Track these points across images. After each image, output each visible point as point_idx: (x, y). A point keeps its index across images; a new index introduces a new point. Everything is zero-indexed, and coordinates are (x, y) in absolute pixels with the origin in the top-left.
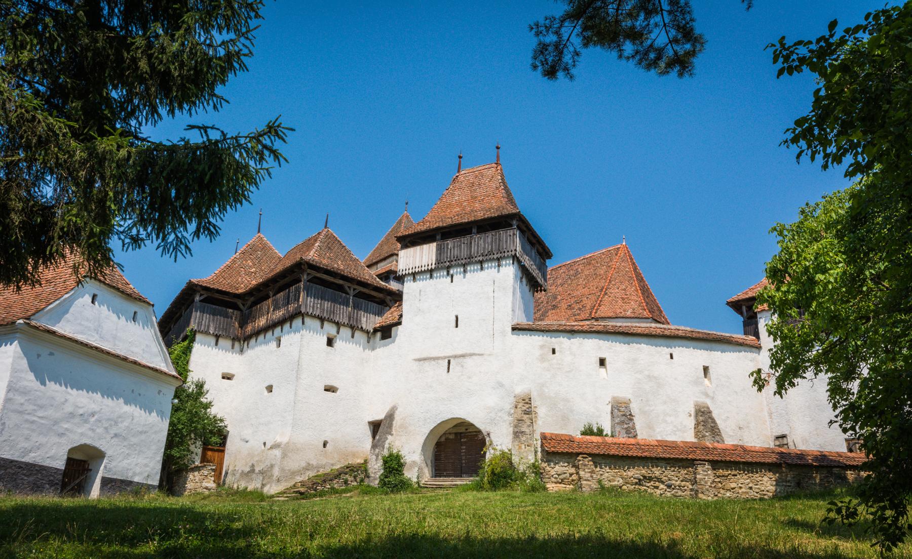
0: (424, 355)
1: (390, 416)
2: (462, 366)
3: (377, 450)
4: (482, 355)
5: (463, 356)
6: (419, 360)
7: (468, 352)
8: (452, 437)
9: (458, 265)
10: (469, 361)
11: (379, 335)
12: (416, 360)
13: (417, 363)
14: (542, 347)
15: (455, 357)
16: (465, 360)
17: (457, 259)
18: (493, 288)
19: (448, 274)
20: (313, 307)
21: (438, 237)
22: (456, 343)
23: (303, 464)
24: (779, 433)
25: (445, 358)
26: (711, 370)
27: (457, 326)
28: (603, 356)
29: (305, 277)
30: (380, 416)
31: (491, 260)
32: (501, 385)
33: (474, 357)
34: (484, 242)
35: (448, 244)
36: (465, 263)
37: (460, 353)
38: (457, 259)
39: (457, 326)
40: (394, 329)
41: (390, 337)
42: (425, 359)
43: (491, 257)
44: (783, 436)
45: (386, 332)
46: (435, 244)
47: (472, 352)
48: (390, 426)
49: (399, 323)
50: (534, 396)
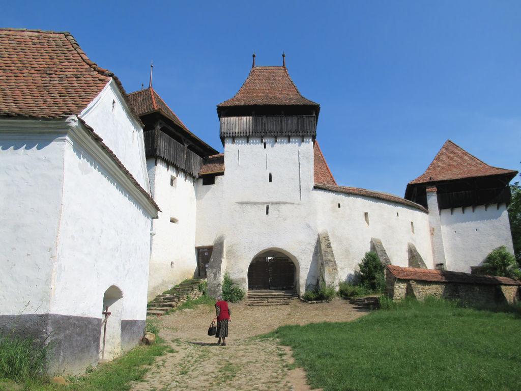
0: (245, 200)
1: (220, 244)
2: (278, 211)
3: (214, 271)
4: (293, 204)
5: (279, 203)
6: (242, 203)
7: (281, 201)
8: (260, 260)
9: (271, 136)
10: (283, 207)
11: (201, 181)
12: (238, 203)
13: (240, 205)
14: (332, 202)
15: (272, 203)
16: (280, 207)
17: (271, 132)
18: (291, 157)
19: (262, 142)
20: (164, 154)
21: (253, 113)
22: (270, 193)
23: (160, 281)
24: (439, 263)
25: (264, 203)
26: (414, 224)
27: (271, 180)
28: (366, 212)
29: (158, 127)
30: (209, 242)
31: (297, 136)
32: (309, 226)
33: (287, 205)
34: (292, 123)
35: (262, 119)
36: (278, 135)
37: (275, 200)
38: (271, 132)
39: (271, 180)
40: (218, 179)
41: (213, 183)
42: (247, 203)
43: (298, 134)
44: (441, 265)
45: (209, 180)
46: (251, 117)
47: (284, 201)
48: (221, 252)
49: (222, 174)
50: (329, 234)
